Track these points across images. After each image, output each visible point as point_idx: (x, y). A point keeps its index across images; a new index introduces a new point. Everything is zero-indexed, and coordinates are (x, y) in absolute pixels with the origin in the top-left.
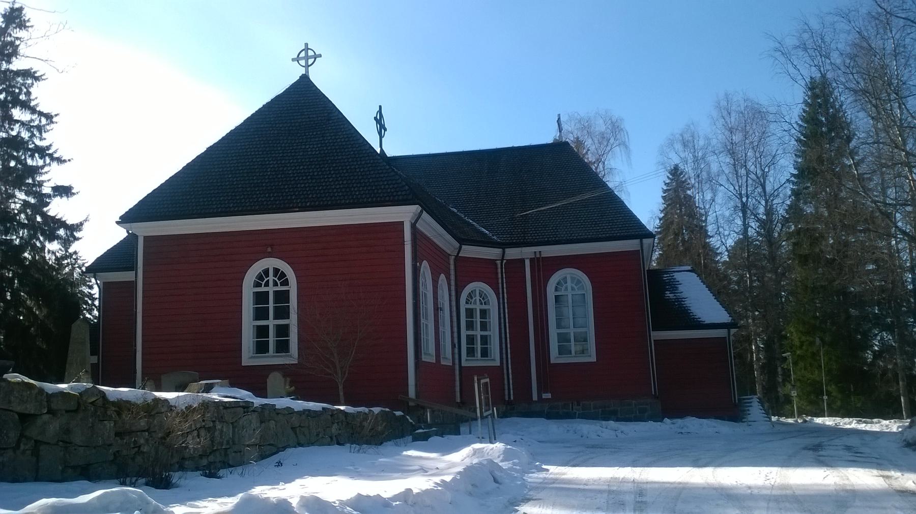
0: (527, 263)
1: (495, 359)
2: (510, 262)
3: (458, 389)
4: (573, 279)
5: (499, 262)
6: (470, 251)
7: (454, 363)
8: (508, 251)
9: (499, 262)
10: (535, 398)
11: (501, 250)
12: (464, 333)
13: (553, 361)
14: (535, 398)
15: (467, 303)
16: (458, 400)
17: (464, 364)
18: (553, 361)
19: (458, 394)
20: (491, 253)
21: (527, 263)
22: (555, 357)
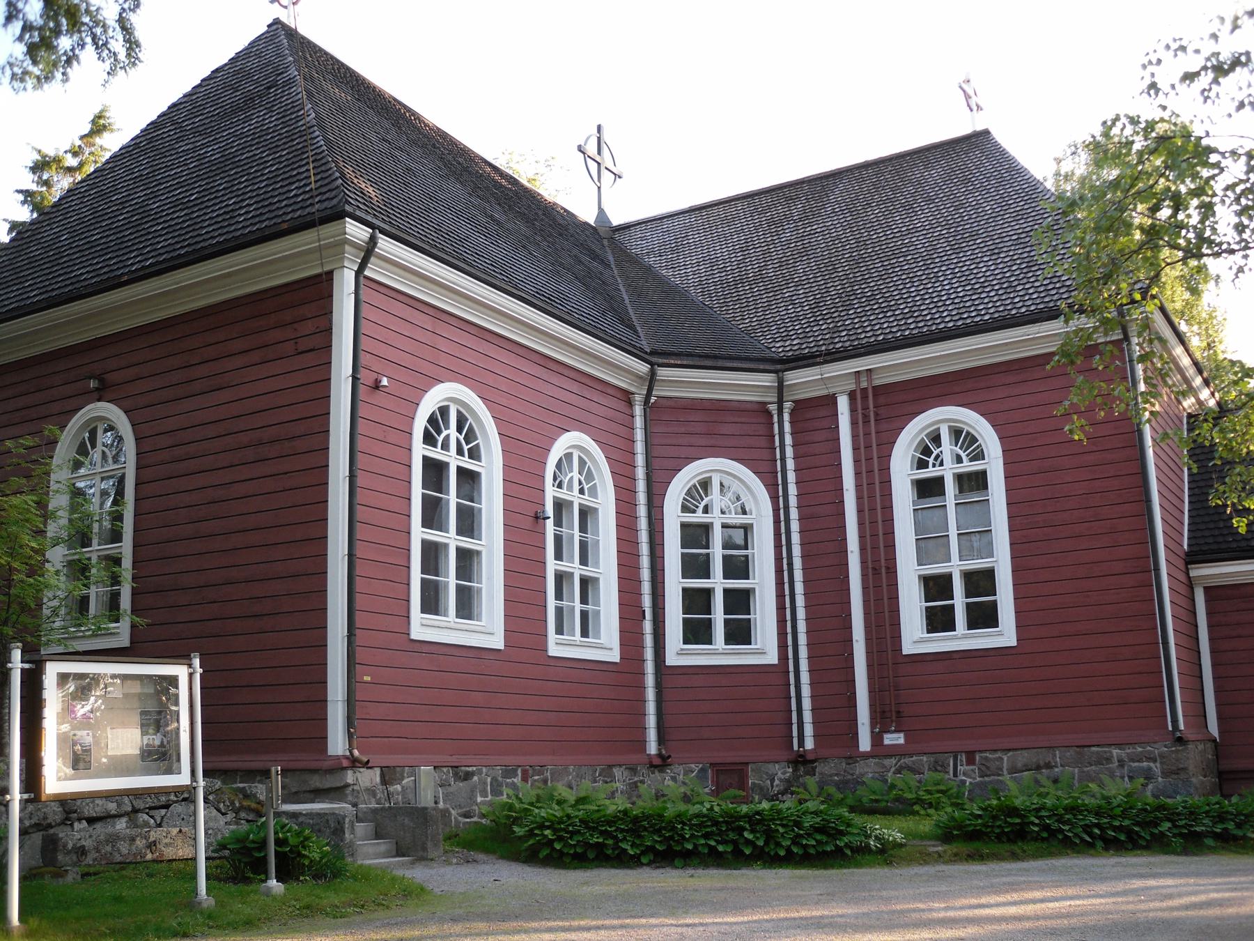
0: (843, 404)
1: (764, 647)
2: (801, 407)
3: (651, 721)
4: (956, 433)
5: (773, 408)
6: (684, 382)
7: (783, 656)
8: (795, 377)
9: (773, 408)
10: (865, 744)
11: (772, 376)
12: (675, 583)
13: (908, 648)
14: (865, 744)
15: (685, 509)
16: (652, 748)
17: (672, 660)
18: (908, 648)
19: (652, 735)
20: (750, 385)
21: (843, 404)
22: (915, 636)
